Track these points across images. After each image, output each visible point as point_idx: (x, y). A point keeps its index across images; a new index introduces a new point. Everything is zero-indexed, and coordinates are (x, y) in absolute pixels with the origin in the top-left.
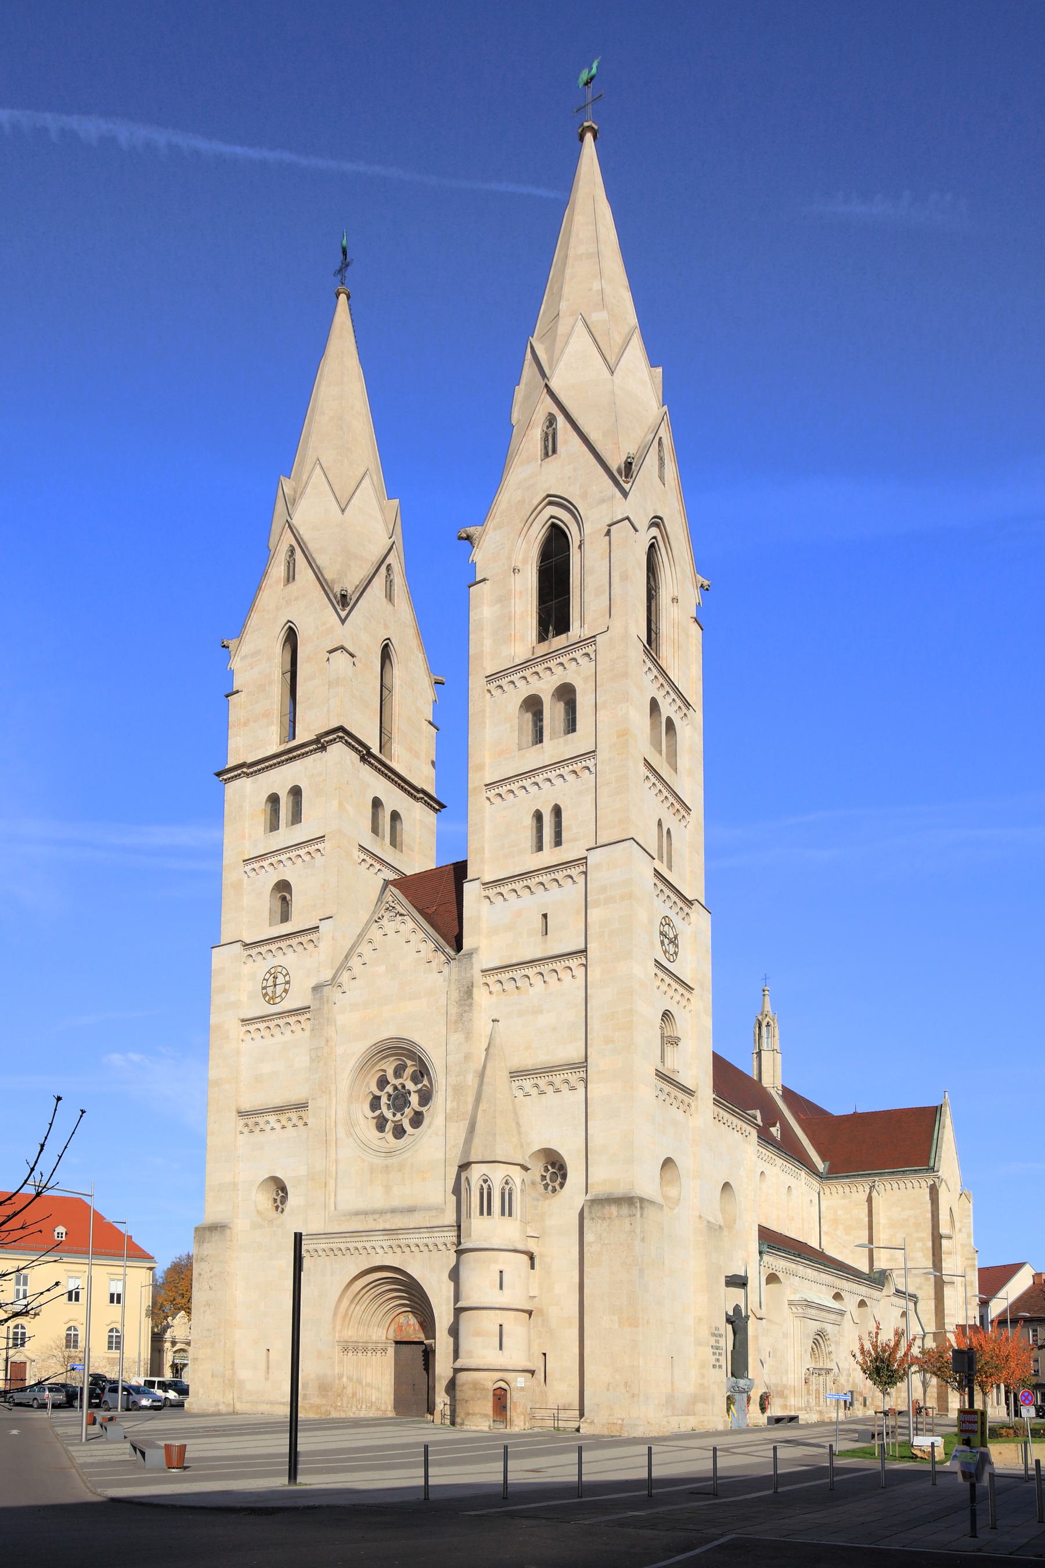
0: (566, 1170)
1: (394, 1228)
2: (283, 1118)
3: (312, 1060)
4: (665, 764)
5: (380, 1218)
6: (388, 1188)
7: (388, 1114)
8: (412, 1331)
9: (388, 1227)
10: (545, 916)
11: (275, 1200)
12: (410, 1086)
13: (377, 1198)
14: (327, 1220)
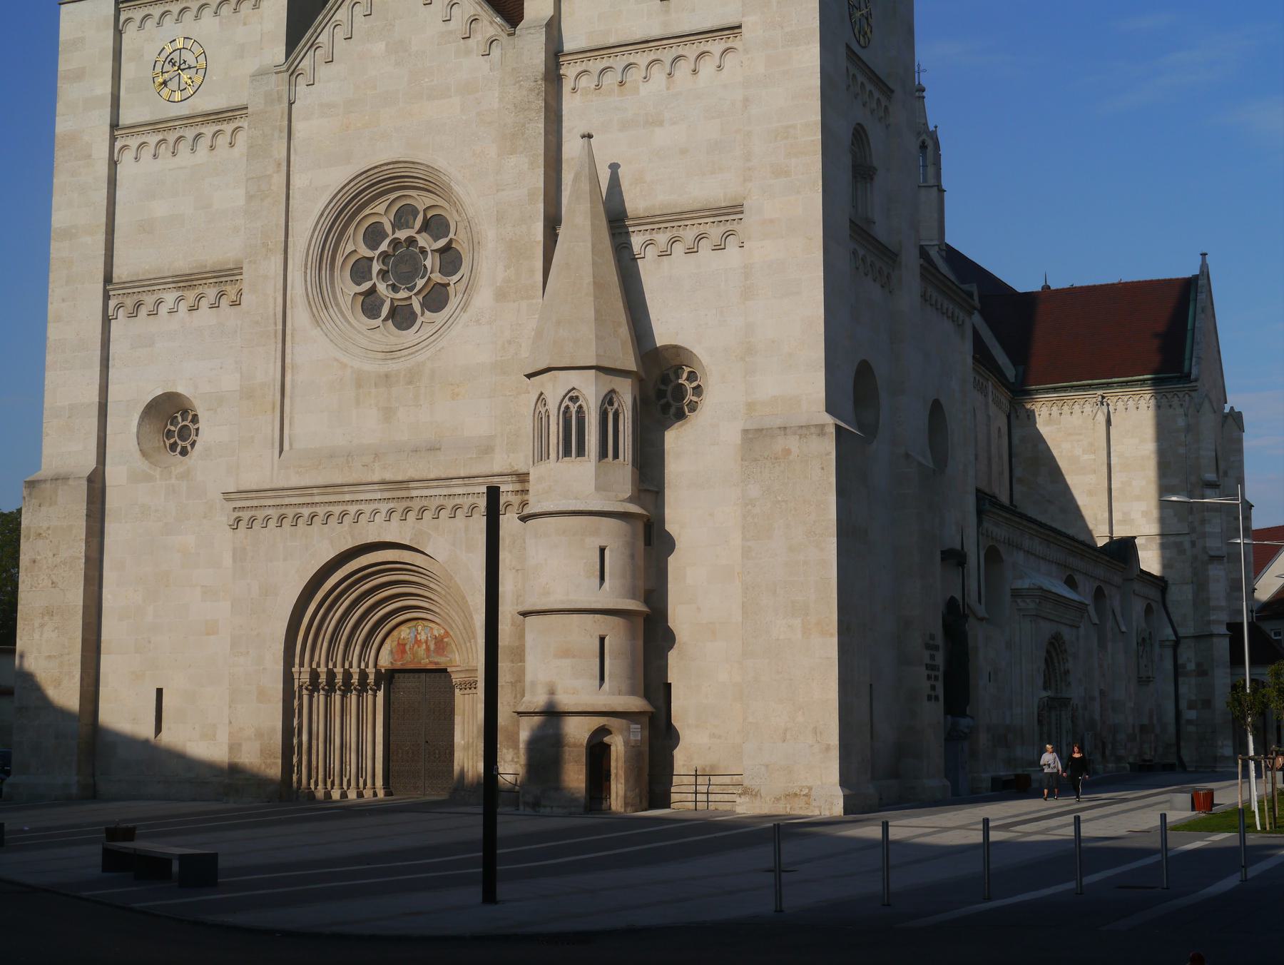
1: (400, 478)
3: (250, 198)
5: (374, 462)
6: (388, 413)
8: (423, 652)
9: (388, 476)
11: (169, 434)
12: (423, 240)
14: (276, 467)
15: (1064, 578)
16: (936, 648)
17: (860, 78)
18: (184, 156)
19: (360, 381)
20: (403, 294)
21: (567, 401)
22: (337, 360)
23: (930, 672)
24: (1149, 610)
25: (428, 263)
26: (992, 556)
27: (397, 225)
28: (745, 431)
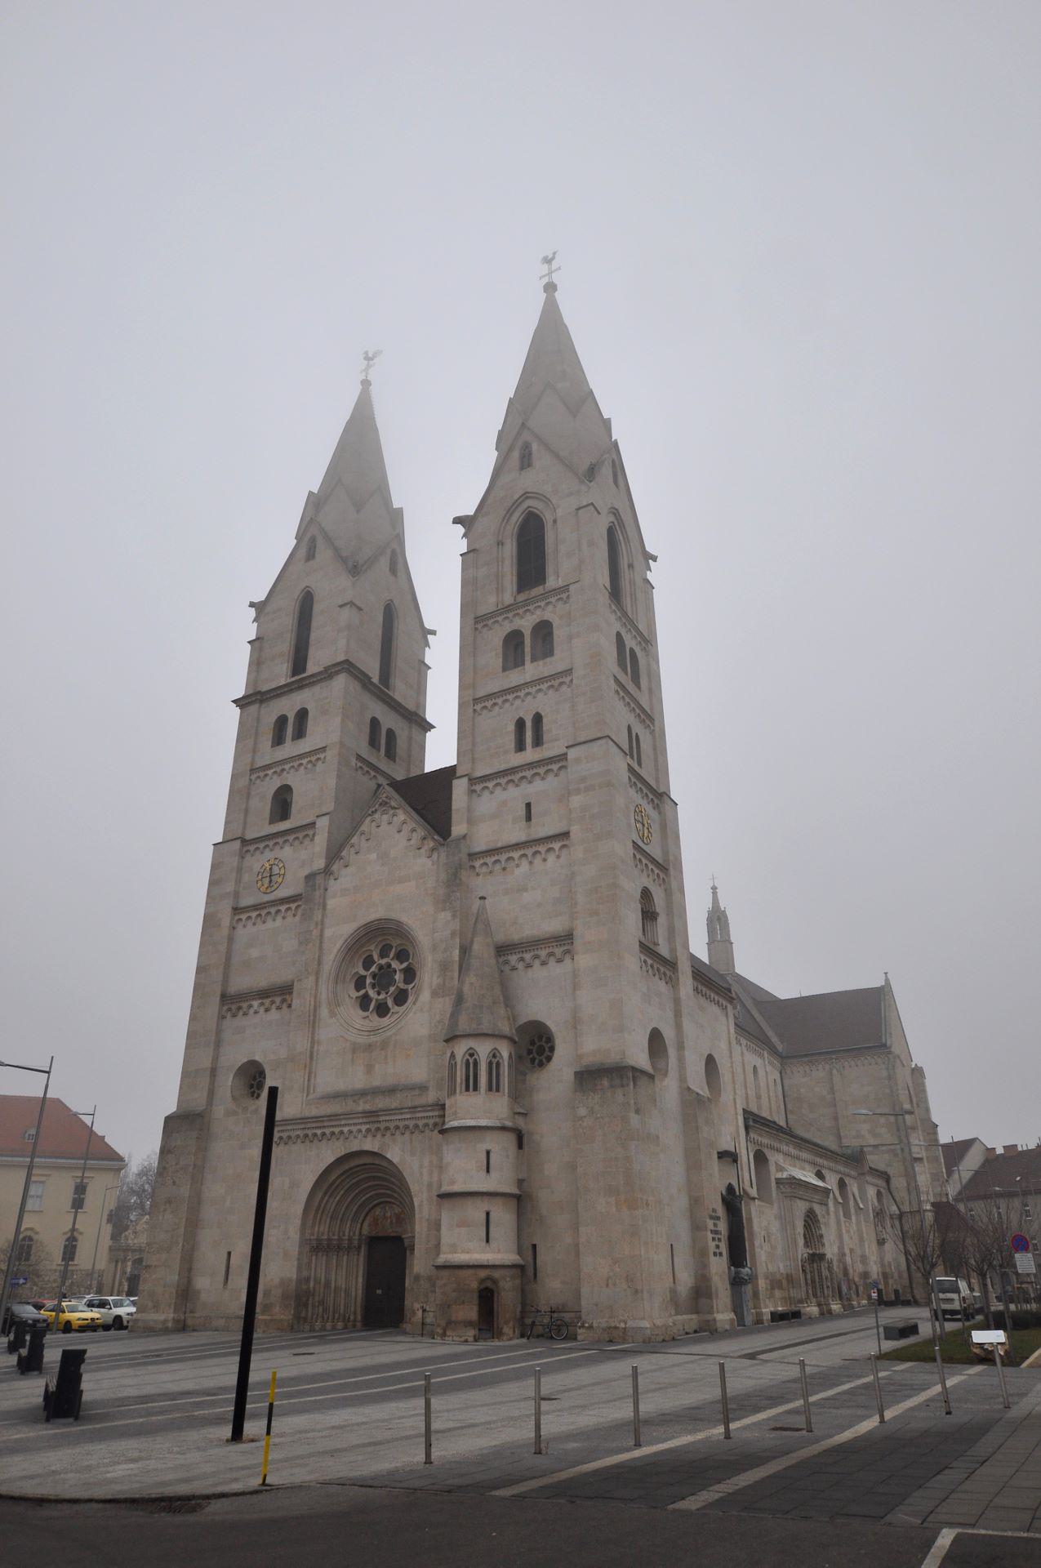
0: (554, 1042)
2: (267, 1002)
3: (301, 943)
4: (631, 682)
6: (369, 1069)
7: (372, 993)
10: (528, 805)
12: (395, 965)
13: (357, 1079)
15: (815, 1171)
16: (718, 1218)
17: (644, 861)
18: (270, 924)
19: (355, 1048)
20: (382, 996)
22: (342, 1037)
23: (714, 1236)
24: (879, 1194)
25: (396, 977)
26: (760, 1159)
27: (382, 956)
28: (576, 1073)
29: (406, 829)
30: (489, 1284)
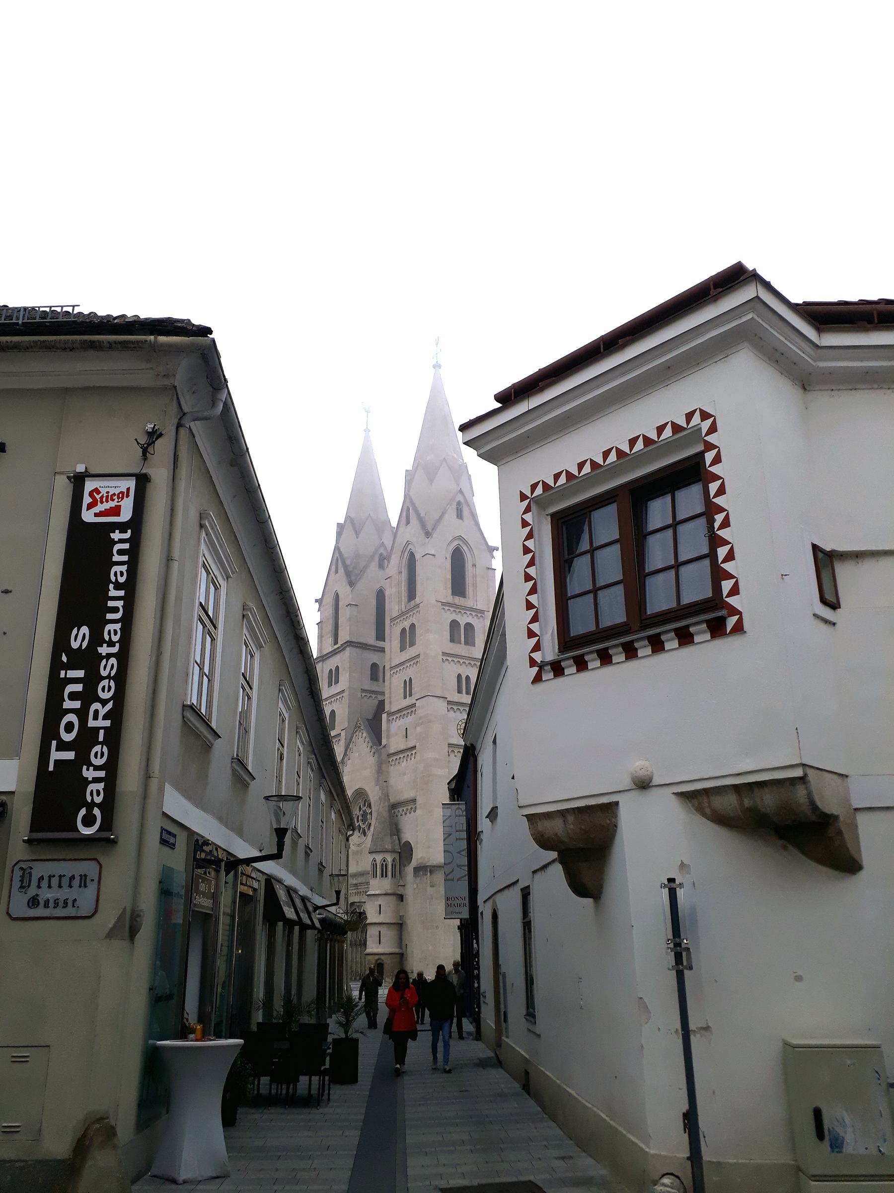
21: (373, 862)
29: (367, 740)
30: (379, 962)
